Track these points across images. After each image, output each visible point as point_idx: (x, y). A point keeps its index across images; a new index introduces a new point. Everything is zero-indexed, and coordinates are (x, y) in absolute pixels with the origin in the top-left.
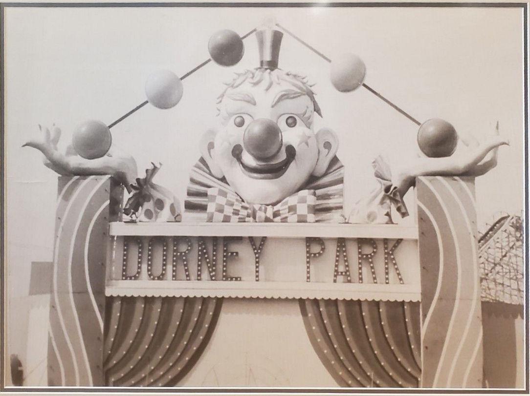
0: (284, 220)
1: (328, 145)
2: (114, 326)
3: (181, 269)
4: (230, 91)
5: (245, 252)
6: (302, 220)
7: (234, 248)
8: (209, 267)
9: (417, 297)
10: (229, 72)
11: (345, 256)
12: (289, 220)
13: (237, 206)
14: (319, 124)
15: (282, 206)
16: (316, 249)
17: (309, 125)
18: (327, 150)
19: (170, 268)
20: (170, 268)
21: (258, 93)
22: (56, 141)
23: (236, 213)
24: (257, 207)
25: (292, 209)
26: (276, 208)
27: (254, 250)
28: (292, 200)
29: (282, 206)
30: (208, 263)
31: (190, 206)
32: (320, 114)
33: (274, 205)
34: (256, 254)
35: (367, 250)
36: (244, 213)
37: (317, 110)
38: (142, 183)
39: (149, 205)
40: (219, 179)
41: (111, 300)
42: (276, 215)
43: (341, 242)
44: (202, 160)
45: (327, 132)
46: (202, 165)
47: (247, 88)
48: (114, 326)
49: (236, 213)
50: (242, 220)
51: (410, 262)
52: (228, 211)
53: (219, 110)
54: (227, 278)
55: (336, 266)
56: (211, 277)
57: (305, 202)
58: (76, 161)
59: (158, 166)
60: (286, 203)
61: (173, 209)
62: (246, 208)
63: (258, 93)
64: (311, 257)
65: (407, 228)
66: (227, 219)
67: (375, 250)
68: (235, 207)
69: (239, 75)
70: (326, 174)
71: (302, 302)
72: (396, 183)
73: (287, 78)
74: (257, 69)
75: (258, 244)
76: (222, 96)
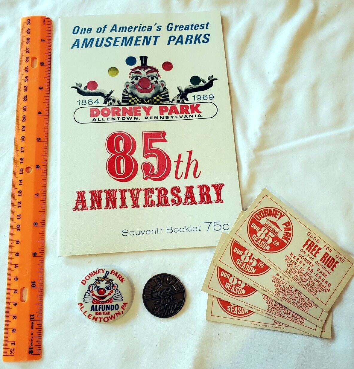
14: (160, 79)
17: (157, 78)
23: (138, 102)
25: (155, 100)
26: (151, 100)
28: (155, 98)
32: (160, 77)
37: (159, 76)
47: (138, 70)
66: (135, 104)
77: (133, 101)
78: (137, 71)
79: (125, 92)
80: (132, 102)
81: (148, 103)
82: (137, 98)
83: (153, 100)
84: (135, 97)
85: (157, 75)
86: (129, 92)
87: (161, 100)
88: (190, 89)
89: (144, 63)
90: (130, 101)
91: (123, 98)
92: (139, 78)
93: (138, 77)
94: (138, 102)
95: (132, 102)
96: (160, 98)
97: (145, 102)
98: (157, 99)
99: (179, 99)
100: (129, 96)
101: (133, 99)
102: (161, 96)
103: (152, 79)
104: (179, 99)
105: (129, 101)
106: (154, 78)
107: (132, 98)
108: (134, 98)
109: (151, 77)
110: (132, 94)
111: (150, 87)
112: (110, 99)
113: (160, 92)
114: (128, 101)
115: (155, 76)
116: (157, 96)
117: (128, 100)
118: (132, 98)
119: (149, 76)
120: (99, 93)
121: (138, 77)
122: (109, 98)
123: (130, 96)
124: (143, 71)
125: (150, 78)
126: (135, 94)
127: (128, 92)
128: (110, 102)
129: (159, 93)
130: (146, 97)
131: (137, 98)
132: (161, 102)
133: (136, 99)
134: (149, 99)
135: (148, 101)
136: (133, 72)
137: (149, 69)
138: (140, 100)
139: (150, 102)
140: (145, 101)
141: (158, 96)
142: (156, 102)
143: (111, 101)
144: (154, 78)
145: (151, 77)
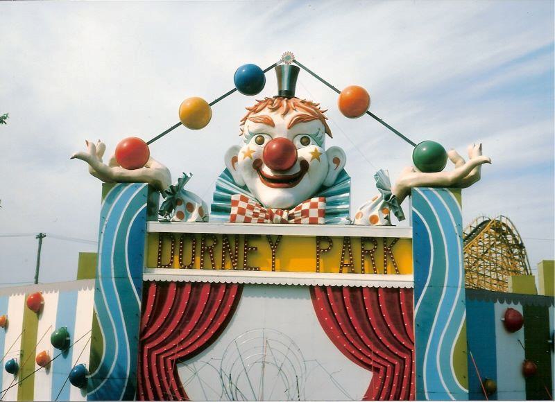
0: (298, 222)
1: (337, 161)
2: (150, 305)
3: (208, 261)
4: (252, 115)
5: (264, 249)
6: (313, 221)
7: (254, 244)
8: (232, 259)
9: (410, 285)
10: (251, 101)
11: (350, 252)
12: (302, 221)
13: (257, 210)
14: (329, 143)
15: (296, 210)
16: (325, 245)
17: (320, 144)
18: (336, 165)
19: (198, 259)
20: (198, 259)
21: (276, 117)
22: (101, 153)
23: (256, 215)
24: (274, 210)
25: (305, 213)
26: (291, 212)
27: (271, 245)
28: (306, 206)
29: (296, 210)
30: (231, 255)
31: (216, 210)
33: (289, 209)
34: (272, 249)
35: (369, 247)
36: (262, 215)
37: (328, 132)
38: (175, 189)
39: (180, 208)
40: (240, 187)
41: (148, 283)
42: (290, 217)
43: (347, 241)
44: (227, 171)
45: (336, 149)
46: (226, 175)
47: (266, 112)
48: (150, 305)
50: (261, 221)
51: (406, 258)
52: (249, 213)
53: (242, 131)
54: (247, 268)
55: (342, 259)
56: (234, 267)
57: (317, 207)
58: (118, 170)
59: (189, 176)
60: (300, 208)
61: (201, 211)
62: (264, 212)
63: (276, 117)
64: (320, 252)
65: (403, 229)
66: (248, 220)
67: (376, 250)
68: (255, 211)
69: (261, 102)
70: (334, 185)
71: (312, 288)
72: (394, 192)
73: (301, 105)
74: (276, 97)
75: (275, 242)
76: (245, 119)
77: (242, 212)
91: (216, 199)
94: (256, 215)
95: (241, 218)
98: (311, 210)
99: (376, 212)
104: (376, 212)
114: (227, 211)
121: (265, 136)
128: (177, 211)
133: (251, 208)
135: (285, 215)
142: (307, 220)
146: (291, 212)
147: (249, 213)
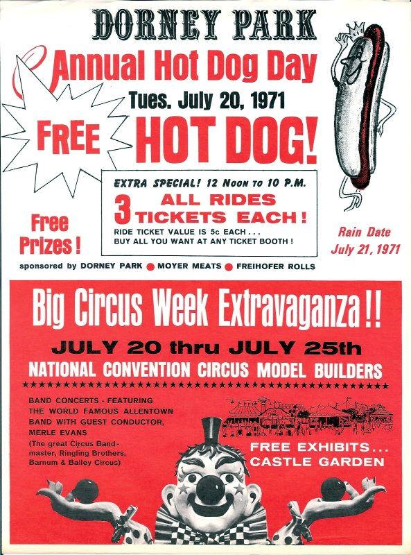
13: (193, 534)
23: (192, 539)
25: (233, 536)
26: (221, 536)
28: (233, 530)
47: (196, 455)
49: (192, 539)
60: (228, 532)
63: (205, 458)
77: (181, 536)
78: (193, 459)
79: (164, 512)
80: (178, 540)
81: (215, 543)
82: (190, 530)
83: (227, 537)
84: (187, 527)
85: (243, 469)
86: (173, 513)
87: (247, 536)
88: (318, 511)
89: (211, 436)
90: (174, 535)
92: (199, 478)
93: (195, 474)
95: (178, 540)
96: (246, 530)
97: (209, 539)
99: (290, 534)
100: (172, 523)
101: (181, 531)
102: (248, 526)
103: (230, 479)
104: (290, 534)
105: (171, 535)
106: (234, 477)
107: (179, 529)
108: (184, 528)
109: (226, 475)
110: (179, 518)
111: (223, 501)
112: (127, 530)
113: (246, 515)
114: (168, 537)
115: (237, 472)
116: (239, 525)
117: (168, 533)
118: (179, 529)
119: (222, 474)
120: (101, 511)
121: (195, 474)
122: (125, 525)
123: (176, 524)
124: (209, 456)
125: (223, 478)
126: (187, 519)
127: (170, 514)
129: (242, 517)
130: (210, 526)
131: (190, 530)
132: (246, 541)
134: (219, 533)
135: (217, 538)
136: (184, 461)
137: (224, 455)
138: (197, 536)
139: (222, 539)
140: (210, 537)
141: (241, 525)
142: (235, 541)
143: (129, 535)
144: (234, 477)
145: (226, 475)
146: (221, 536)
147: (187, 537)
